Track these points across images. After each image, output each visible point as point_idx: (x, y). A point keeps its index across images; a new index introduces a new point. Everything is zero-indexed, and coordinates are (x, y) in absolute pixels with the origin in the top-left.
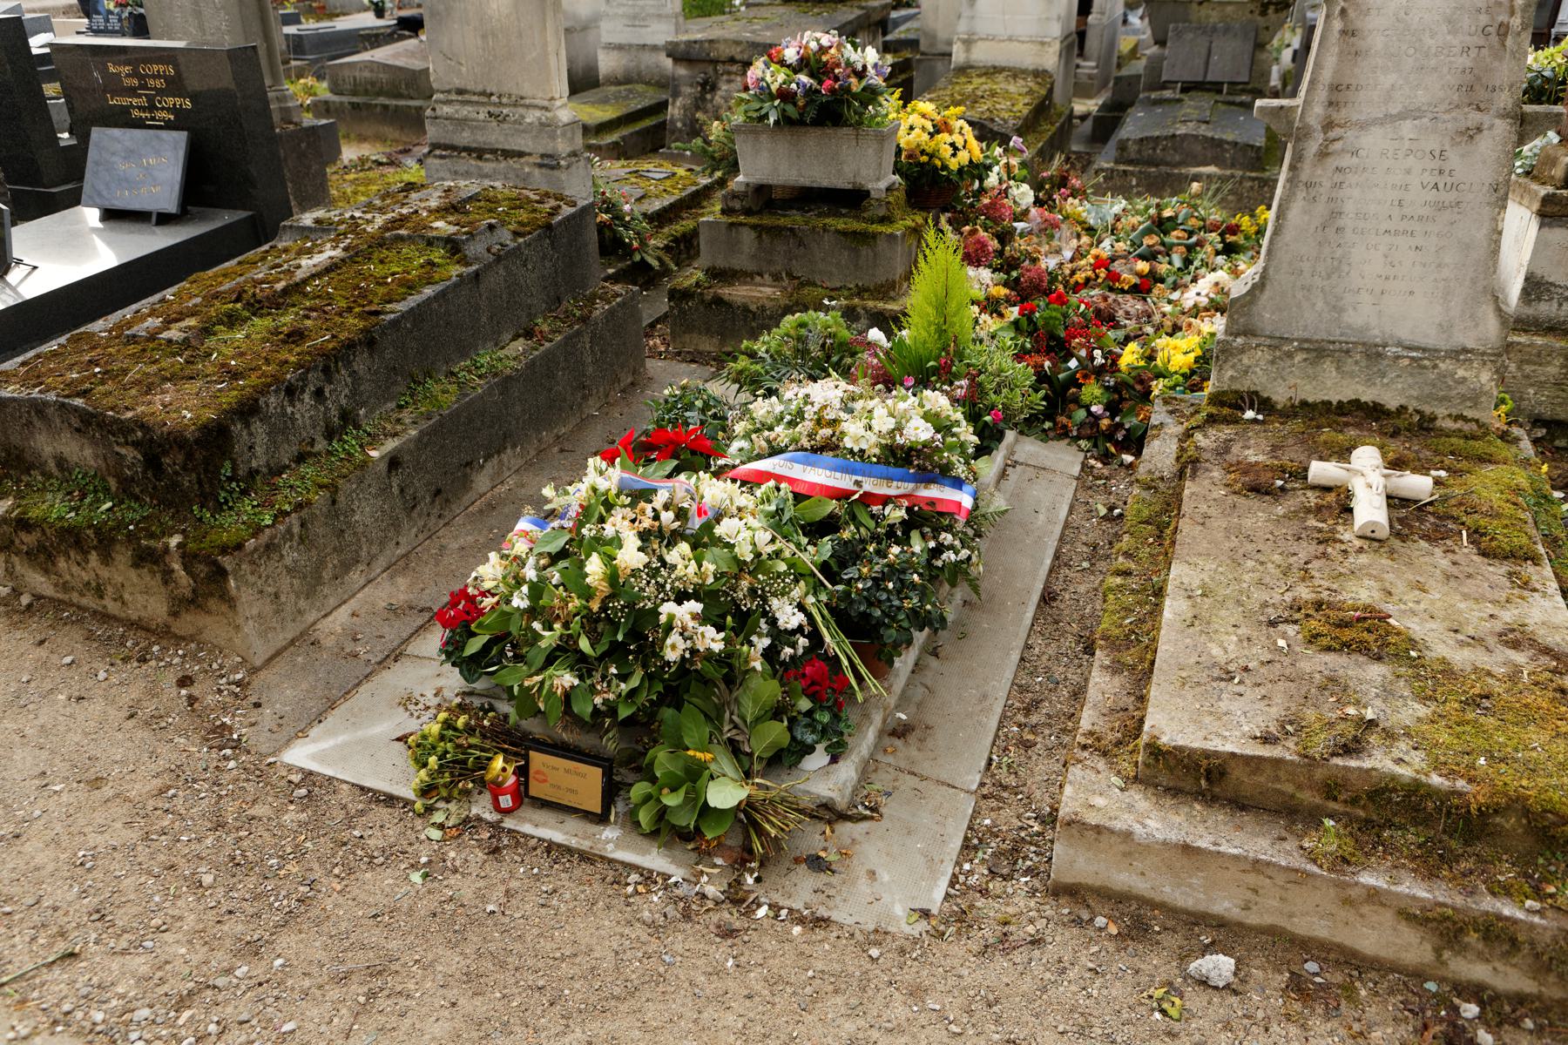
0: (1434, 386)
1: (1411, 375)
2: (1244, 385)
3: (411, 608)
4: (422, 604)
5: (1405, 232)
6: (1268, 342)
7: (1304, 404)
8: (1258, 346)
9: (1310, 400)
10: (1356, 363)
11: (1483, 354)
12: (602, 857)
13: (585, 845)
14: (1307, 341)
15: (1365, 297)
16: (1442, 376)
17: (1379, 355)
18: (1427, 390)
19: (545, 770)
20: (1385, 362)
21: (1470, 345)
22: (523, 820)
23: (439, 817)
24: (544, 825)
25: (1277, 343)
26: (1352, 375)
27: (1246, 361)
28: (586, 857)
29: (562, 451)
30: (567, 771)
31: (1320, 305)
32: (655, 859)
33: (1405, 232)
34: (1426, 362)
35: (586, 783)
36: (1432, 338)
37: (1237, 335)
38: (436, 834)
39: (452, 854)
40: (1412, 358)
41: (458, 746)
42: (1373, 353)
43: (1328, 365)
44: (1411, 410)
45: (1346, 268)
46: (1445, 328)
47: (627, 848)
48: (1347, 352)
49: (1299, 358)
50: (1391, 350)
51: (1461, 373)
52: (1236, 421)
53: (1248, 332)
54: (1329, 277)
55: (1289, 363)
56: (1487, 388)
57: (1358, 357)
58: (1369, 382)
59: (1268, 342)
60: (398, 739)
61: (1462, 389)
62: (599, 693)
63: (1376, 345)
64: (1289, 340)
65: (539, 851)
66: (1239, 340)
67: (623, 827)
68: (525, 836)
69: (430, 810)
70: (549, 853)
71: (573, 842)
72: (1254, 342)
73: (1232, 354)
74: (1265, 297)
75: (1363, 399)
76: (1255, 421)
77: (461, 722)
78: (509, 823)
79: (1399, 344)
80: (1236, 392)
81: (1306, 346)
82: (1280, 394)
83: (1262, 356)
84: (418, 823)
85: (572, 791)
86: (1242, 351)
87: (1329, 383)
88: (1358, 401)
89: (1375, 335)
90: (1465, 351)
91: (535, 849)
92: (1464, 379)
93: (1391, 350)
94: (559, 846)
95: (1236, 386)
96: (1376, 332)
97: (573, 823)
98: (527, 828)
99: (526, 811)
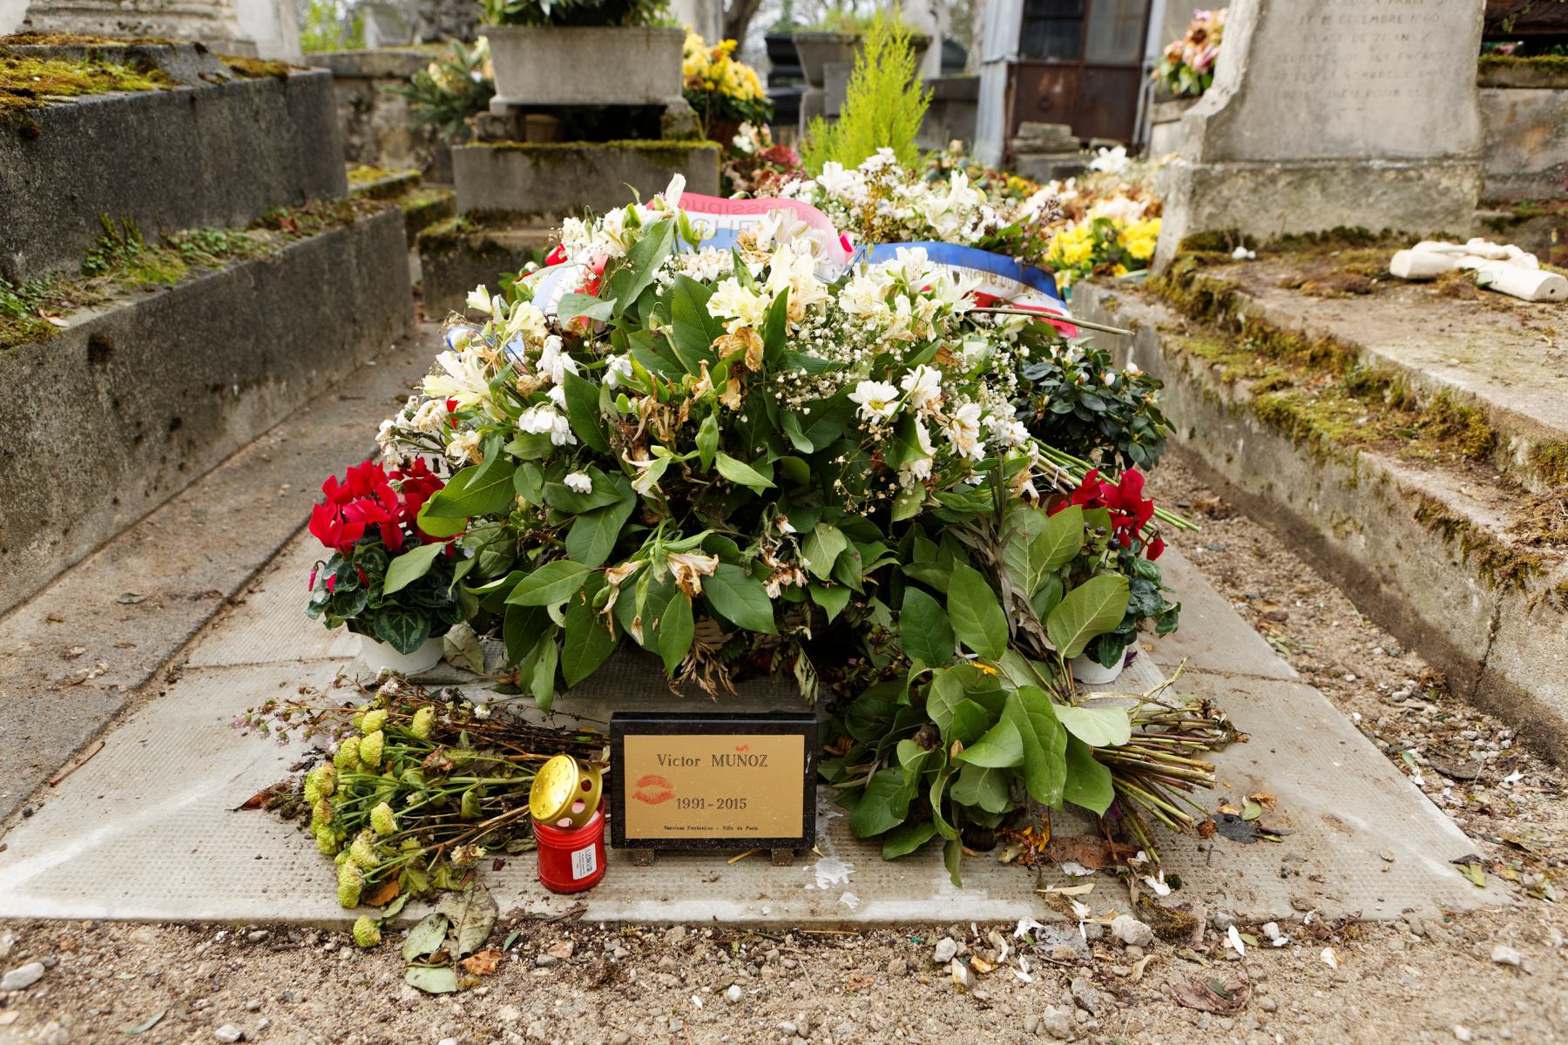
0: (1418, 200)
1: (1397, 190)
2: (1224, 224)
3: (173, 597)
4: (192, 588)
5: (1392, 18)
6: (1249, 166)
7: (1288, 238)
8: (1239, 171)
9: (1294, 233)
10: (1342, 181)
11: (1464, 158)
12: (845, 926)
13: (796, 910)
14: (1289, 161)
15: (1350, 102)
16: (1427, 188)
17: (1366, 170)
18: (1412, 206)
19: (664, 771)
20: (1371, 178)
21: (1452, 150)
22: (624, 896)
23: (425, 940)
24: (681, 893)
25: (1258, 166)
26: (1337, 197)
27: (1226, 193)
28: (812, 936)
29: (343, 398)
30: (719, 761)
31: (1303, 115)
32: (947, 897)
33: (1392, 18)
34: (1412, 173)
35: (763, 775)
36: (1415, 146)
37: (1214, 161)
38: (440, 980)
39: (509, 1013)
40: (1399, 170)
41: (430, 773)
42: (1360, 170)
43: (1313, 188)
44: (1395, 232)
45: (1330, 67)
46: (1429, 132)
47: (883, 892)
48: (1333, 169)
49: (1282, 183)
50: (1376, 164)
51: (1445, 182)
52: (1230, 262)
53: (1226, 157)
54: (1313, 80)
55: (1271, 189)
56: (1469, 197)
57: (1344, 174)
58: (1355, 204)
59: (1249, 166)
60: (250, 805)
61: (1446, 202)
62: (767, 574)
63: (1360, 160)
64: (1273, 163)
65: (702, 950)
66: (1219, 167)
67: (845, 857)
68: (650, 927)
69: (392, 930)
70: (727, 947)
71: (768, 911)
72: (1235, 167)
73: (1211, 187)
74: (1245, 112)
75: (1349, 225)
76: (1247, 259)
77: (421, 721)
78: (600, 910)
79: (1383, 156)
80: (1215, 233)
81: (1290, 166)
82: (1264, 228)
83: (1243, 183)
84: (375, 966)
85: (731, 803)
86: (1222, 180)
87: (1313, 210)
88: (1342, 228)
89: (1359, 147)
90: (1447, 157)
91: (689, 949)
92: (1448, 189)
93: (1376, 164)
94: (740, 927)
95: (1215, 226)
96: (1359, 143)
97: (739, 875)
98: (647, 910)
99: (625, 877)
